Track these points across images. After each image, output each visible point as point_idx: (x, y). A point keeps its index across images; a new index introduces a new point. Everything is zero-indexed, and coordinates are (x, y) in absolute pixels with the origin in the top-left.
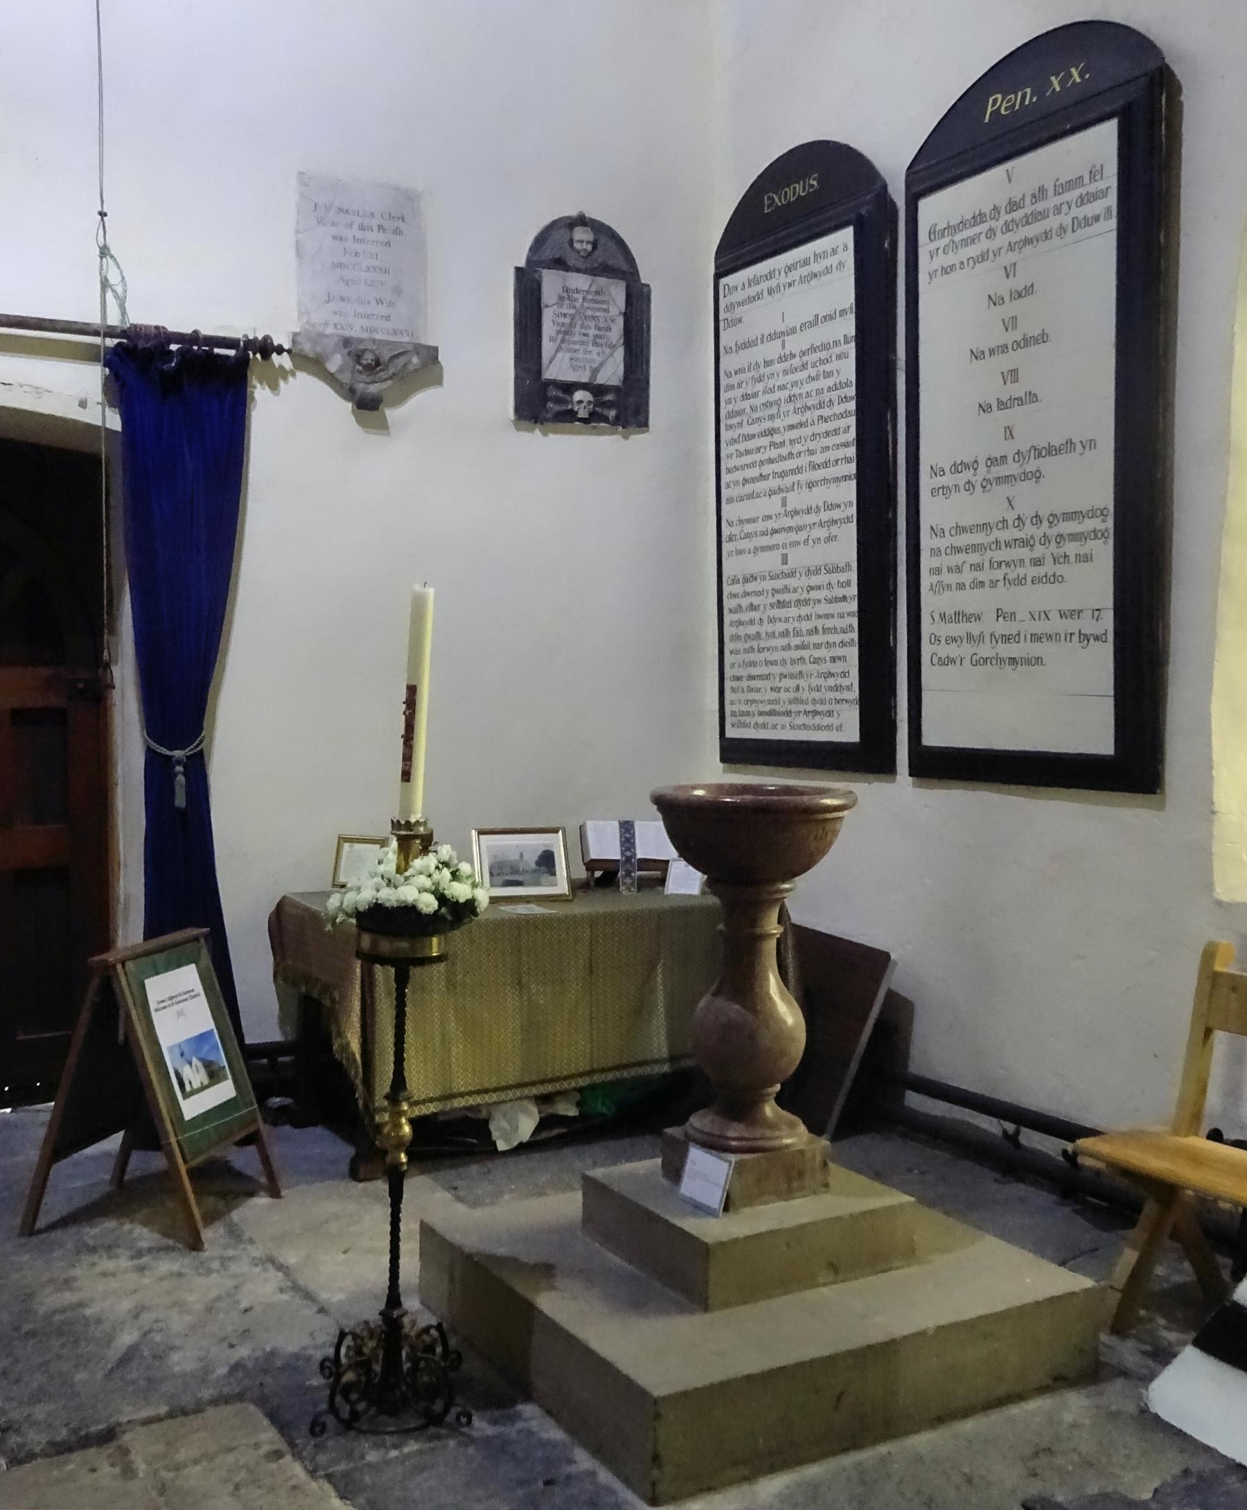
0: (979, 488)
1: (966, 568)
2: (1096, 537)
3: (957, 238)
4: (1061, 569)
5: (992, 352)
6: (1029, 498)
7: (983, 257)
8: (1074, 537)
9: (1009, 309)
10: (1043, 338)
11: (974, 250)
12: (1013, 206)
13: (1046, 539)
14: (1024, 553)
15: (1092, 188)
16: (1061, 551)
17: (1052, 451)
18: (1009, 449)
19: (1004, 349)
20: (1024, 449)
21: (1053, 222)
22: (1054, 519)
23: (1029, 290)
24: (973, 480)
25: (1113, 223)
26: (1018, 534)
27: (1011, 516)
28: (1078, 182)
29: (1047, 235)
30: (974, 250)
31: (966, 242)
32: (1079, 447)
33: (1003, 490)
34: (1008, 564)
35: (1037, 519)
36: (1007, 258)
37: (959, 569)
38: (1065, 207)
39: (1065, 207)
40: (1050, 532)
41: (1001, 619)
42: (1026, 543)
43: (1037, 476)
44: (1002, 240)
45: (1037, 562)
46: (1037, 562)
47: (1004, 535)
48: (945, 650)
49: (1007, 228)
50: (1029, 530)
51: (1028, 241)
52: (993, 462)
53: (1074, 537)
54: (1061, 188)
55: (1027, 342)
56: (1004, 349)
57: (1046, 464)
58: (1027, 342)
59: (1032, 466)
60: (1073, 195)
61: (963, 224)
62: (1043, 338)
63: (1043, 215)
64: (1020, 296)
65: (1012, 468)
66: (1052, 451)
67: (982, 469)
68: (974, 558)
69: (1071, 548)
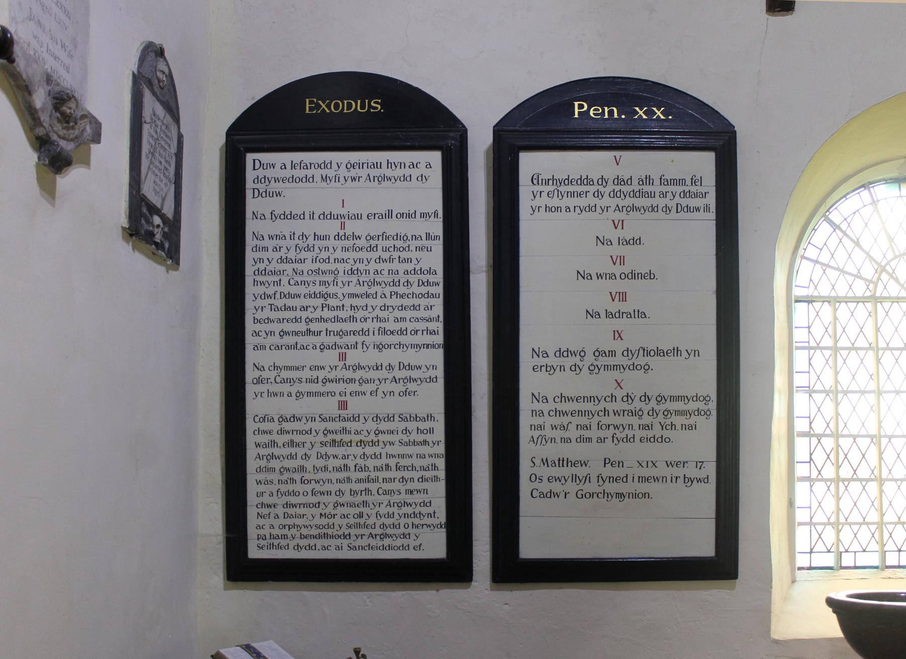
0: (585, 370)
1: (572, 427)
2: (699, 414)
3: (563, 189)
4: (666, 433)
5: (599, 276)
6: (635, 383)
7: (591, 209)
8: (679, 413)
9: (617, 250)
10: (651, 276)
11: (582, 202)
12: (619, 181)
13: (653, 412)
14: (635, 421)
15: (693, 189)
16: (668, 422)
17: (659, 352)
18: (619, 346)
19: (612, 276)
20: (633, 348)
21: (662, 202)
22: (661, 399)
23: (637, 241)
24: (581, 365)
25: (713, 215)
26: (626, 406)
27: (619, 394)
28: (682, 182)
29: (653, 209)
30: (582, 202)
31: (572, 194)
32: (685, 354)
33: (616, 374)
34: (616, 427)
35: (646, 398)
36: (618, 216)
37: (564, 428)
38: (669, 195)
39: (669, 195)
40: (657, 408)
41: (609, 466)
42: (633, 413)
43: (646, 368)
44: (606, 201)
45: (648, 427)
46: (648, 427)
47: (611, 406)
48: (545, 487)
49: (614, 194)
50: (637, 405)
51: (634, 208)
52: (598, 353)
53: (679, 413)
54: (663, 181)
55: (634, 275)
56: (612, 276)
57: (653, 361)
58: (634, 275)
59: (642, 360)
60: (678, 189)
61: (569, 181)
62: (651, 276)
63: (651, 195)
64: (628, 243)
65: (619, 360)
66: (659, 352)
67: (589, 359)
68: (583, 420)
69: (678, 420)
